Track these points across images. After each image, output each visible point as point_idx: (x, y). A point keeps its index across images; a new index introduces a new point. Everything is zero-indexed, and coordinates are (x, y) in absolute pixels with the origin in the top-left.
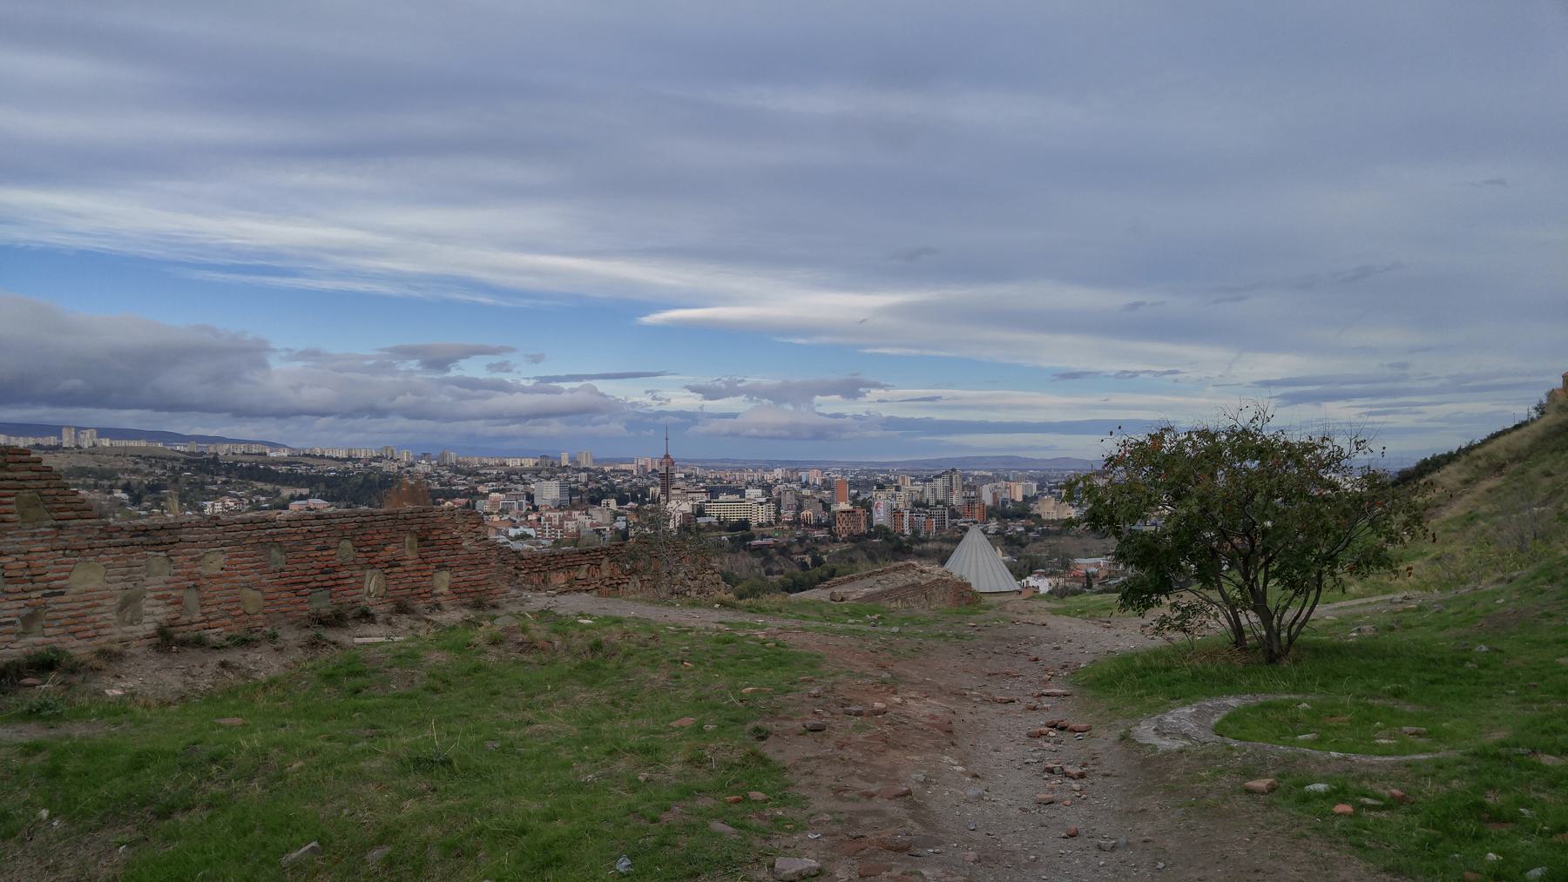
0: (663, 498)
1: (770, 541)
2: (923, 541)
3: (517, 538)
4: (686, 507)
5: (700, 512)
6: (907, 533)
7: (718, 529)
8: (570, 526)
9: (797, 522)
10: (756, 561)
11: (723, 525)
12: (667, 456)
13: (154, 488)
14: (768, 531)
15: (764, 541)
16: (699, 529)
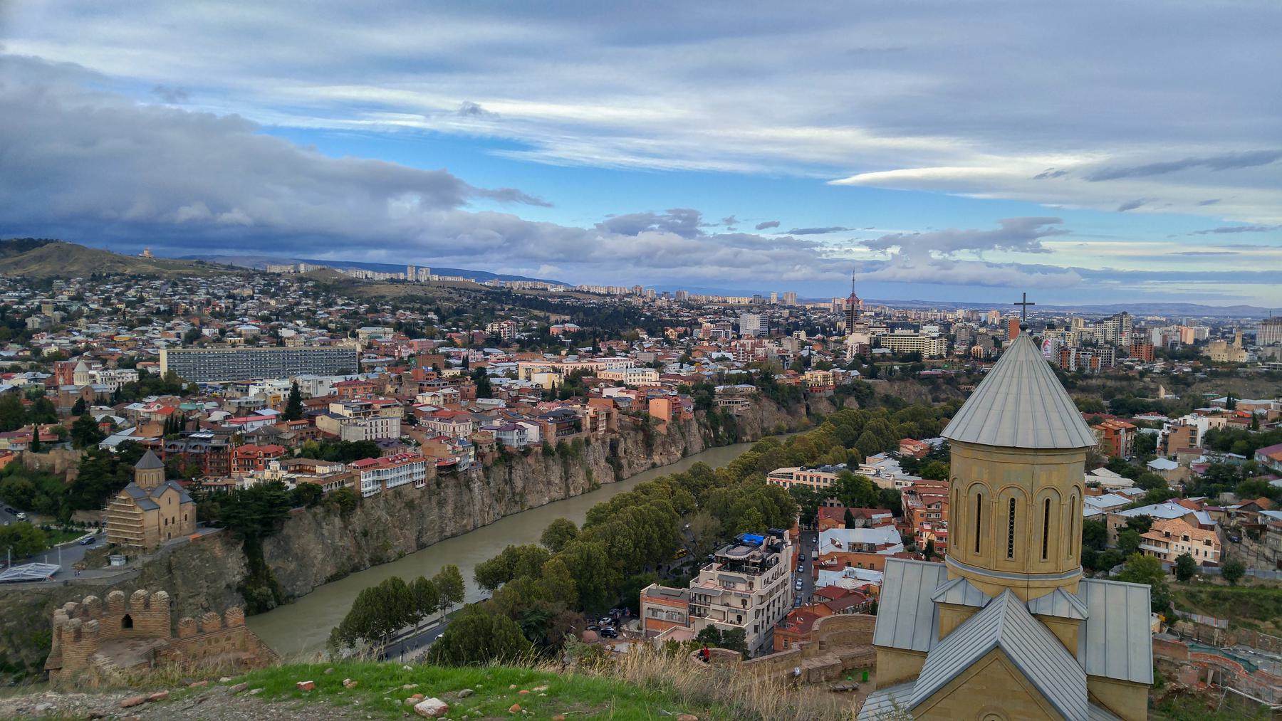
0: (847, 331)
1: (939, 372)
2: (1087, 377)
3: (718, 360)
4: (865, 340)
5: (876, 343)
6: (1073, 368)
7: (890, 359)
8: (760, 352)
9: (967, 356)
10: (924, 389)
11: (896, 356)
12: (853, 295)
13: (459, 312)
14: (938, 362)
15: (933, 372)
16: (874, 359)
